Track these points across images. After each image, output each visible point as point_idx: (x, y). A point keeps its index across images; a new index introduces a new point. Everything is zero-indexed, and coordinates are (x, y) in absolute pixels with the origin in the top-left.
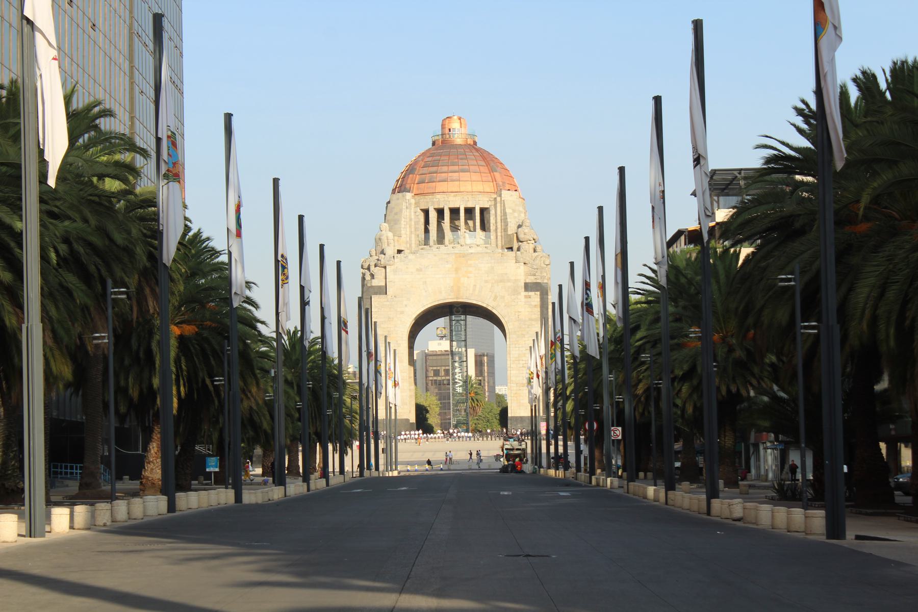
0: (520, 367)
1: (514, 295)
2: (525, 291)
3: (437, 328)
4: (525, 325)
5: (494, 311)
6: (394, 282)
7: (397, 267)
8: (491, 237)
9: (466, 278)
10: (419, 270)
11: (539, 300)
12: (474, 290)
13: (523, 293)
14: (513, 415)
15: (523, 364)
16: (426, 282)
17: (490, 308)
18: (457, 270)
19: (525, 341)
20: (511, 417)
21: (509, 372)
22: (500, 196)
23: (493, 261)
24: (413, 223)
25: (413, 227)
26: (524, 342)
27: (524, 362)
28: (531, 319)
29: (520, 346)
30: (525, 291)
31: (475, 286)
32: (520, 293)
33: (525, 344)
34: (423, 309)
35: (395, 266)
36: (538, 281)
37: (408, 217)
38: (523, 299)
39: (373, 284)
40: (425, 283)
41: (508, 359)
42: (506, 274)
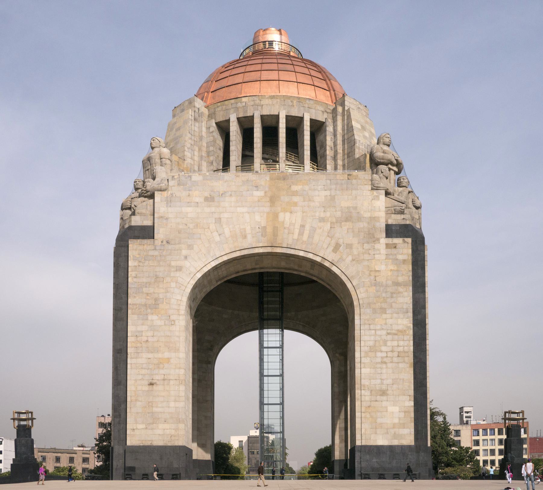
0: (377, 363)
1: (368, 243)
3: (255, 423)
4: (386, 292)
5: (334, 269)
6: (167, 219)
7: (172, 194)
8: (328, 166)
9: (288, 214)
10: (209, 199)
11: (410, 251)
12: (301, 234)
13: (384, 240)
15: (382, 358)
16: (220, 218)
17: (327, 264)
18: (273, 200)
19: (386, 319)
20: (361, 446)
22: (343, 104)
23: (333, 187)
24: (205, 144)
25: (204, 149)
27: (384, 355)
29: (378, 327)
30: (386, 237)
31: (303, 226)
32: (378, 240)
33: (386, 324)
34: (214, 264)
35: (169, 192)
36: (408, 222)
37: (197, 134)
39: (133, 224)
40: (219, 221)
41: (357, 348)
42: (355, 208)
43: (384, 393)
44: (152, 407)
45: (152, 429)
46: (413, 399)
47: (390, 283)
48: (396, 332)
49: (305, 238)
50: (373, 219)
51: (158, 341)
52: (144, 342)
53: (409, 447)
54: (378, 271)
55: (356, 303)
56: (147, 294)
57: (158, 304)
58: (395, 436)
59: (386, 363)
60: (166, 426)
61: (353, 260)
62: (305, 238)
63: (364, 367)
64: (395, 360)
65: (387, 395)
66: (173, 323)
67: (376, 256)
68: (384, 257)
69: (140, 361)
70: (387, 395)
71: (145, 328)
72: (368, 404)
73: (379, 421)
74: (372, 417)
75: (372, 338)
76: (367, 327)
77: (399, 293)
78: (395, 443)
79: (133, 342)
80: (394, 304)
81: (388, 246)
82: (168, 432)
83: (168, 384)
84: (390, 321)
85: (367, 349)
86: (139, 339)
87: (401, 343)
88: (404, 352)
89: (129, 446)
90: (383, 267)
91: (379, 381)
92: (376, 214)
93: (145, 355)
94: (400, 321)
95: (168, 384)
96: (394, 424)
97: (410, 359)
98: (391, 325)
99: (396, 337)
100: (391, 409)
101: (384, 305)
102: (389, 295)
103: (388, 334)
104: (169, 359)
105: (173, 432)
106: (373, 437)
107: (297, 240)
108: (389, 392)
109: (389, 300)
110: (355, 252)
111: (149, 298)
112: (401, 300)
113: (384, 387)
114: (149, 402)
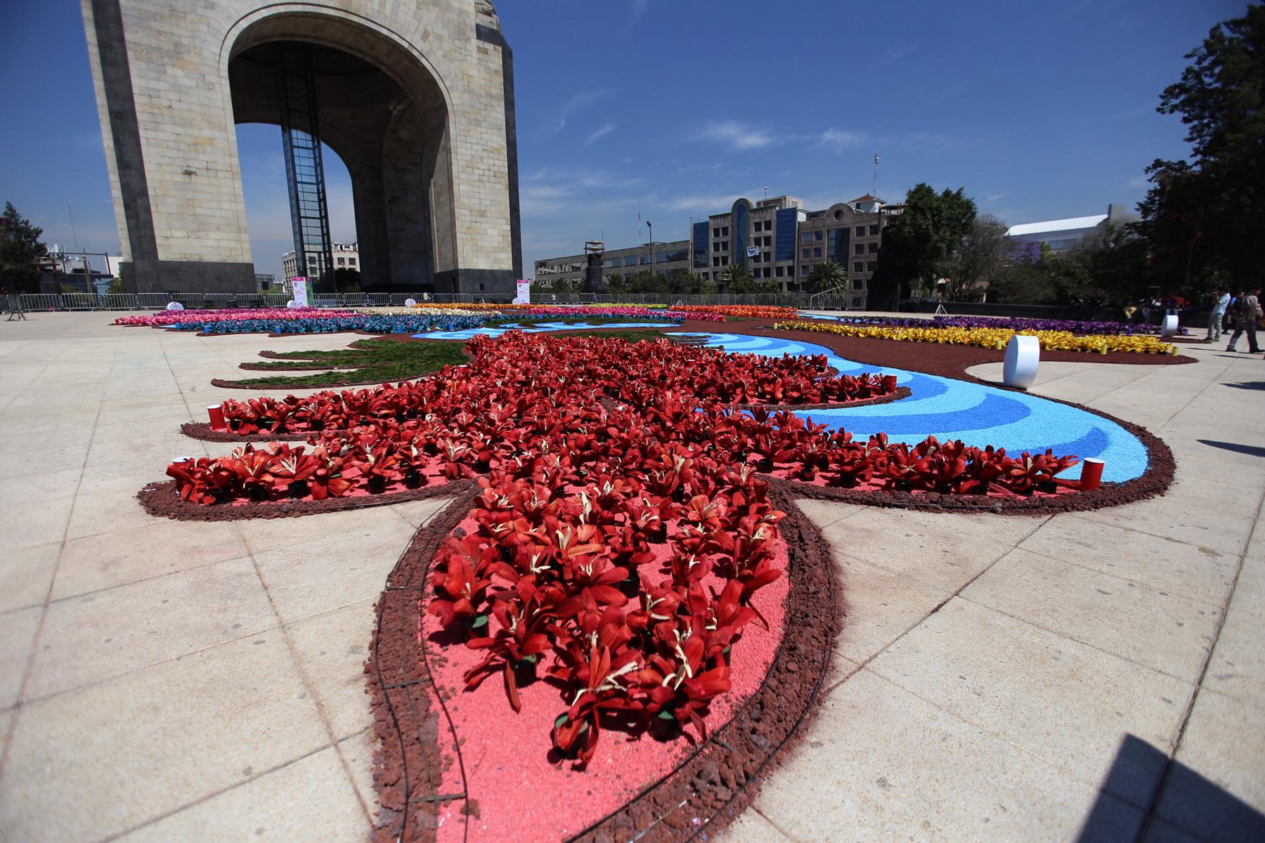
0: (474, 181)
1: (459, 40)
2: (479, 37)
5: (423, 61)
11: (501, 62)
13: (475, 42)
14: (466, 267)
15: (479, 175)
20: (465, 270)
21: (455, 187)
26: (479, 136)
28: (490, 96)
29: (474, 141)
30: (478, 38)
32: (468, 39)
33: (481, 138)
36: (495, 28)
38: (475, 54)
43: (482, 214)
44: (195, 207)
45: (198, 238)
46: (509, 223)
47: (483, 93)
48: (490, 149)
49: (388, 11)
50: (462, 12)
51: (189, 110)
52: (165, 107)
53: (509, 271)
54: (471, 76)
55: (449, 108)
56: (160, 32)
57: (182, 53)
58: (496, 261)
59: (483, 182)
60: (220, 235)
61: (444, 56)
62: (388, 11)
63: (463, 184)
64: (492, 179)
65: (486, 216)
66: (210, 86)
67: (468, 58)
68: (476, 62)
69: (162, 136)
70: (486, 216)
71: (162, 86)
72: (468, 225)
73: (480, 243)
74: (472, 239)
75: (469, 152)
76: (463, 138)
77: (492, 106)
78: (496, 267)
79: (145, 104)
80: (488, 118)
81: (479, 49)
82: (225, 244)
83: (216, 176)
84: (485, 137)
85: (464, 163)
86: (154, 101)
87: (497, 162)
88: (499, 172)
89: (164, 262)
90: (475, 73)
91: (477, 201)
92: (466, 7)
93: (169, 128)
94: (494, 138)
95: (216, 176)
96: (494, 248)
97: (505, 180)
98: (487, 141)
99: (492, 155)
100: (490, 232)
101: (478, 117)
102: (483, 107)
103: (484, 150)
104: (211, 141)
105: (233, 244)
106: (475, 260)
107: (379, 11)
108: (488, 214)
109: (483, 112)
110: (446, 46)
111: (160, 38)
112: (494, 115)
113: (483, 208)
114: (187, 200)
